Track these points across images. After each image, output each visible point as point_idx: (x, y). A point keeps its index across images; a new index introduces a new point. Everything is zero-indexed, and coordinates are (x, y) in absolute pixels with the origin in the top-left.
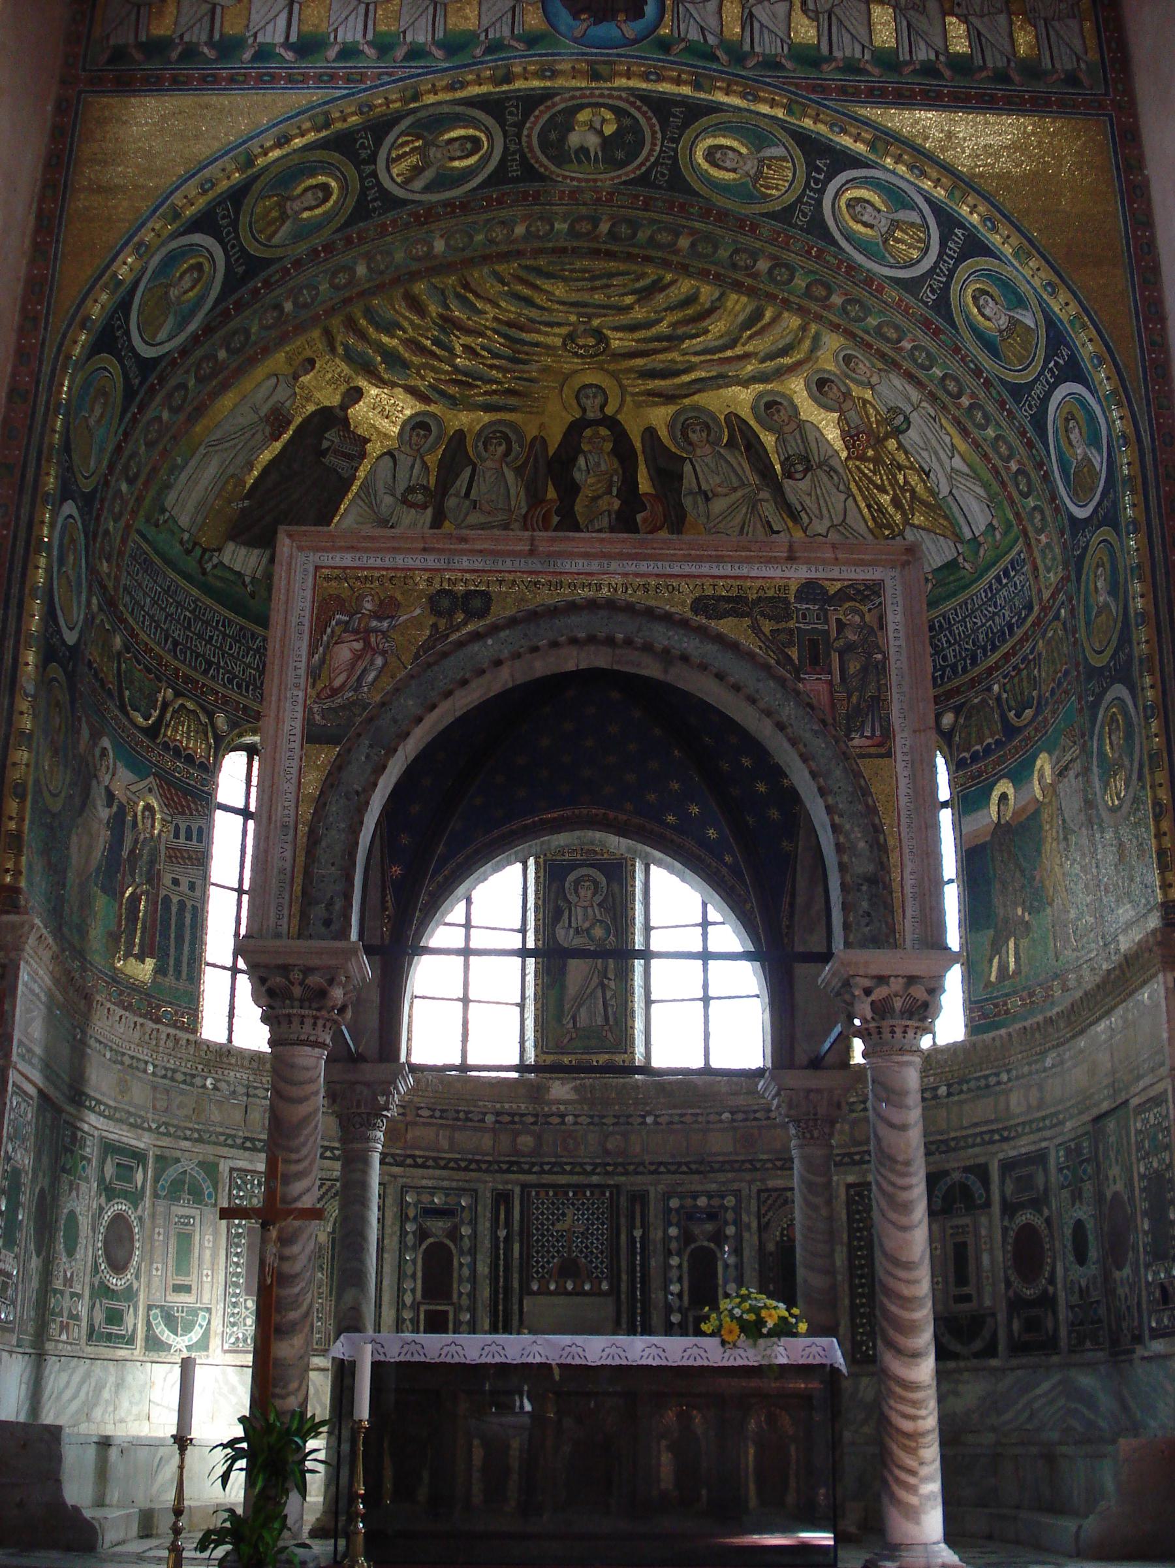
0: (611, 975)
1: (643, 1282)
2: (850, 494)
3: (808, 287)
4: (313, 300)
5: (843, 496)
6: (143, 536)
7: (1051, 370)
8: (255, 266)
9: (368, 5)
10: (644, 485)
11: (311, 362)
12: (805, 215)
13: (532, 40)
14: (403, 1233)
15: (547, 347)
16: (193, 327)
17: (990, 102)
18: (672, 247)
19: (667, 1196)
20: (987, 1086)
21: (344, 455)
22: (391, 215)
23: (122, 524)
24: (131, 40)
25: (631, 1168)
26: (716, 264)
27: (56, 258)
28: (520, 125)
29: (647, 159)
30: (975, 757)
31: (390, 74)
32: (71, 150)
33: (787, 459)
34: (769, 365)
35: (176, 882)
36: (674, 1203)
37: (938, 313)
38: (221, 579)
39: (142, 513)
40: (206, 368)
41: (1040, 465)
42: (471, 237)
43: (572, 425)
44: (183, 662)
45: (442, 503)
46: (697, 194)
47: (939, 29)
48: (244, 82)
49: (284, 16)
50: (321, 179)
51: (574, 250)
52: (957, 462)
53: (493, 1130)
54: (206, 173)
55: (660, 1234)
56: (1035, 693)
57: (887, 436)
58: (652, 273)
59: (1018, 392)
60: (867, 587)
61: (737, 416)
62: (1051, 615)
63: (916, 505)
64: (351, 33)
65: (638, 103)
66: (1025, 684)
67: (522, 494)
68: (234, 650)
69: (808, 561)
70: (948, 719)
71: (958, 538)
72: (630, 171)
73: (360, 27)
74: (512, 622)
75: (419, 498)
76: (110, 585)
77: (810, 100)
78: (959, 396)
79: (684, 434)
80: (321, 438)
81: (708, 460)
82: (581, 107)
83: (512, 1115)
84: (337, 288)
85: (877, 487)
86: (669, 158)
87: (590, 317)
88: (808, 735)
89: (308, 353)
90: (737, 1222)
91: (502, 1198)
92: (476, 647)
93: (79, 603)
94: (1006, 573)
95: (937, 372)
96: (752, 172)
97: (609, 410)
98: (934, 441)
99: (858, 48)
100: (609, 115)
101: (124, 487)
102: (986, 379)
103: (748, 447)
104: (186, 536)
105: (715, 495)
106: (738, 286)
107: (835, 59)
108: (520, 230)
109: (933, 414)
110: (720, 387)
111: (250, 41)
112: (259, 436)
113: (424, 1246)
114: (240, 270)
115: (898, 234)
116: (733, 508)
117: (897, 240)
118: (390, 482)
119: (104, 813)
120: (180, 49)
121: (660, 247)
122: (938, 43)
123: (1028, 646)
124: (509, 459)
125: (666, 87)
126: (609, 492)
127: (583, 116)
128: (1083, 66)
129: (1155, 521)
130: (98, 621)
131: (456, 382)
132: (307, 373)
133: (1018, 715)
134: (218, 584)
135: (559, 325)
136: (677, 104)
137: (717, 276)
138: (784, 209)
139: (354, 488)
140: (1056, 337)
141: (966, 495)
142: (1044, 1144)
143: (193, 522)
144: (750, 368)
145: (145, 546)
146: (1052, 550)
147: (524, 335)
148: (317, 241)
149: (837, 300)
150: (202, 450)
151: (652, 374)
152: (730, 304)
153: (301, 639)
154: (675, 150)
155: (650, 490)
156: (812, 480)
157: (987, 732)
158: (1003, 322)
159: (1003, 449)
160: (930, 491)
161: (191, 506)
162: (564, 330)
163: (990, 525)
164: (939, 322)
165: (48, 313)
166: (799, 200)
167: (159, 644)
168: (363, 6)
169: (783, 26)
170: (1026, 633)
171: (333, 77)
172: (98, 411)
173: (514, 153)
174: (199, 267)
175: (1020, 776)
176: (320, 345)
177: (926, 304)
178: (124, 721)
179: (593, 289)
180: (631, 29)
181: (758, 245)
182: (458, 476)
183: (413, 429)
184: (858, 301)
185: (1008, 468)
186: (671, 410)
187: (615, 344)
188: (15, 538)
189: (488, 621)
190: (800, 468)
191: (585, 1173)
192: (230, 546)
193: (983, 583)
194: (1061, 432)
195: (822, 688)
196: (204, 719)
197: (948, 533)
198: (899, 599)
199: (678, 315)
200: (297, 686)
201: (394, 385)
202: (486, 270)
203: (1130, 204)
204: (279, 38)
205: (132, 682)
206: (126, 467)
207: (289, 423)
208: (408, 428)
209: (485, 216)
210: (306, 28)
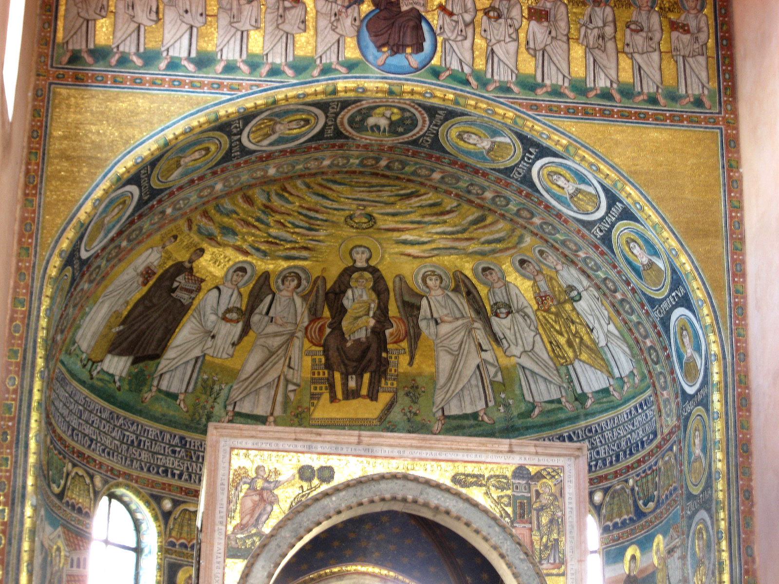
2: (538, 333)
3: (518, 210)
5: (533, 334)
8: (154, 193)
9: (242, 32)
10: (393, 310)
11: (175, 237)
12: (519, 174)
13: (351, 66)
15: (333, 222)
17: (644, 118)
18: (428, 177)
21: (186, 290)
22: (244, 158)
24: (84, 47)
26: (456, 188)
27: (39, 206)
28: (337, 114)
29: (418, 133)
31: (258, 86)
32: (46, 127)
33: (496, 304)
34: (487, 248)
37: (604, 243)
38: (101, 380)
39: (64, 348)
41: (665, 349)
42: (294, 167)
43: (346, 270)
44: (77, 442)
46: (449, 153)
47: (614, 65)
48: (160, 85)
49: (186, 37)
51: (361, 173)
52: (612, 328)
54: (138, 151)
56: (656, 493)
57: (565, 302)
59: (653, 302)
60: (554, 471)
61: (462, 273)
63: (583, 349)
64: (231, 53)
65: (416, 106)
66: (650, 485)
67: (306, 314)
68: (107, 428)
69: (520, 453)
70: (598, 497)
71: (611, 374)
72: (407, 137)
74: (347, 486)
75: (234, 316)
77: (529, 115)
78: (615, 291)
81: (440, 298)
82: (379, 106)
87: (365, 207)
88: (517, 562)
89: (175, 233)
92: (326, 501)
94: (641, 405)
95: (601, 275)
96: (487, 147)
97: (373, 263)
98: (597, 313)
99: (561, 77)
100: (395, 110)
103: (469, 293)
105: (443, 322)
106: (470, 202)
107: (545, 86)
108: (326, 163)
109: (597, 295)
110: (452, 254)
111: (165, 54)
112: (135, 285)
114: (146, 198)
116: (455, 331)
117: (579, 199)
118: (215, 305)
120: (117, 57)
121: (419, 176)
122: (613, 73)
123: (653, 460)
125: (436, 102)
127: (378, 111)
128: (706, 92)
129: (731, 411)
131: (267, 242)
132: (171, 242)
134: (100, 384)
135: (343, 210)
137: (457, 195)
138: (506, 169)
139: (190, 312)
140: (677, 282)
141: (617, 349)
143: (89, 346)
144: (473, 247)
147: (317, 215)
148: (195, 176)
149: (537, 221)
150: (100, 300)
152: (463, 211)
153: (223, 494)
155: (398, 315)
156: (512, 321)
157: (624, 510)
158: (645, 260)
160: (593, 341)
161: (89, 336)
162: (347, 213)
165: (36, 245)
166: (517, 165)
168: (239, 33)
169: (513, 60)
170: (652, 451)
171: (220, 86)
174: (124, 202)
175: (645, 544)
176: (185, 228)
177: (596, 236)
179: (369, 192)
180: (415, 60)
181: (486, 184)
182: (262, 301)
183: (235, 271)
184: (551, 225)
185: (645, 343)
186: (416, 264)
187: (381, 224)
188: (21, 400)
189: (333, 484)
190: (504, 310)
192: (109, 357)
193: (625, 408)
194: (678, 336)
195: (526, 532)
196: (88, 480)
197: (604, 370)
198: (573, 479)
199: (428, 211)
200: (221, 523)
201: (225, 245)
202: (299, 183)
203: (730, 192)
204: (184, 54)
207: (154, 273)
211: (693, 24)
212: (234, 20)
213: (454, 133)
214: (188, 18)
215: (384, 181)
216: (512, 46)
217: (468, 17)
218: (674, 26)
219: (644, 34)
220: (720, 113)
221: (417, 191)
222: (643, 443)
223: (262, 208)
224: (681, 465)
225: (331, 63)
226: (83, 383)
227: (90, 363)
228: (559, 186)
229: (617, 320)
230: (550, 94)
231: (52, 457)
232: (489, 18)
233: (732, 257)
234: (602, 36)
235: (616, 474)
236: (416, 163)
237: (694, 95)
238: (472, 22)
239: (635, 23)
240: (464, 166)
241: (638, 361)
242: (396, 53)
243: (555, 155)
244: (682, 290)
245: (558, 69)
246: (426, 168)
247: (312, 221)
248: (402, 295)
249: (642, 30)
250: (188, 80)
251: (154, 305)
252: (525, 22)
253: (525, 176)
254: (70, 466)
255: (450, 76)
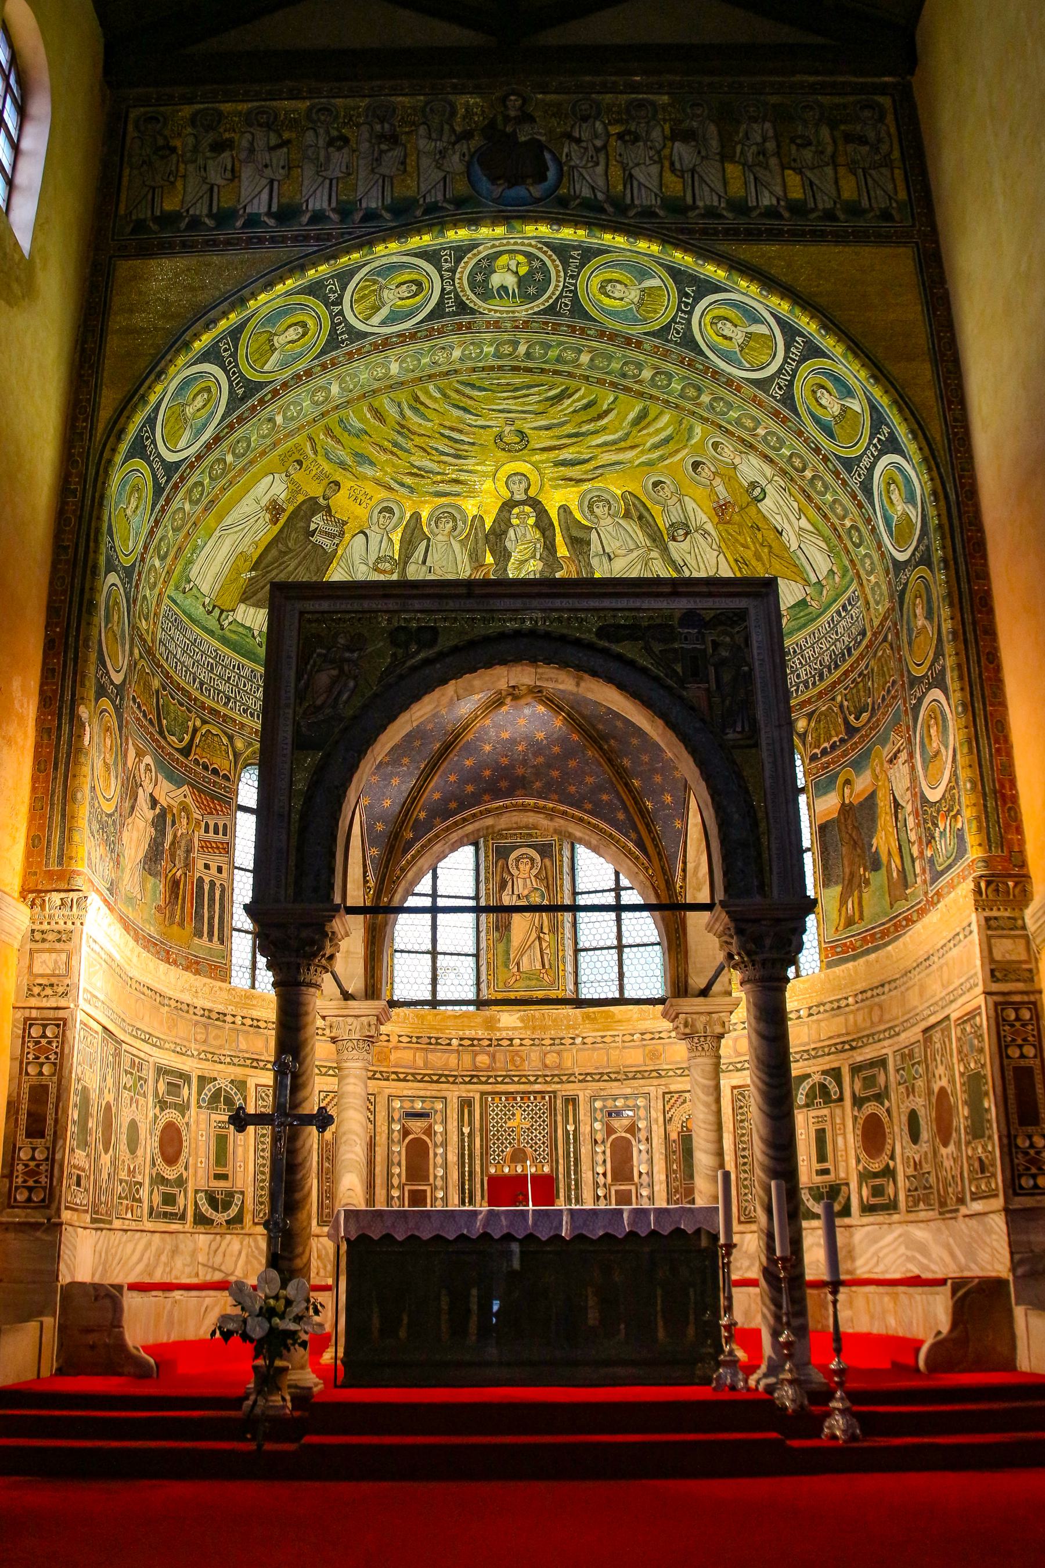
0: (546, 930)
1: (576, 1165)
4: (299, 414)
5: (716, 553)
6: (174, 601)
7: (875, 446)
9: (331, 180)
11: (300, 463)
12: (678, 333)
13: (459, 202)
14: (390, 1131)
16: (207, 435)
19: (593, 1099)
20: (839, 1007)
23: (157, 591)
25: (564, 1078)
28: (453, 271)
29: (553, 293)
30: (824, 752)
31: (350, 233)
35: (207, 867)
36: (598, 1104)
40: (218, 469)
43: (504, 504)
45: (404, 569)
46: (595, 320)
49: (266, 191)
50: (301, 318)
52: (804, 523)
53: (458, 1051)
55: (588, 1129)
56: (869, 700)
58: (561, 384)
59: (849, 464)
62: (881, 638)
64: (319, 202)
68: (248, 687)
71: (807, 582)
72: (539, 304)
73: (326, 198)
76: (149, 639)
78: (804, 470)
79: (590, 507)
80: (309, 521)
81: (610, 528)
82: (500, 254)
83: (472, 1039)
84: (316, 404)
85: (743, 546)
86: (571, 291)
87: (513, 421)
89: (297, 457)
90: (649, 1119)
91: (466, 1103)
93: (124, 652)
94: (844, 607)
96: (636, 300)
97: (532, 493)
98: (786, 508)
99: (715, 198)
100: (521, 258)
101: (157, 563)
102: (824, 456)
103: (641, 517)
104: (207, 600)
106: (627, 389)
107: (698, 208)
108: (457, 353)
113: (407, 1141)
114: (241, 391)
115: (752, 343)
119: (150, 815)
123: (862, 664)
124: (455, 533)
126: (534, 557)
128: (894, 205)
130: (139, 667)
133: (857, 719)
134: (234, 637)
136: (575, 248)
137: (613, 384)
141: (812, 548)
142: (884, 1051)
145: (175, 608)
146: (879, 587)
147: (463, 437)
148: (300, 367)
149: (705, 398)
150: (217, 534)
151: (564, 463)
154: (575, 285)
157: (833, 733)
158: (836, 410)
159: (839, 511)
163: (831, 571)
164: (786, 412)
166: (673, 320)
167: (188, 683)
168: (327, 182)
169: (656, 183)
171: (306, 238)
172: (133, 503)
173: (449, 293)
177: (774, 398)
178: (163, 742)
179: (515, 398)
180: (537, 191)
181: (642, 357)
190: (681, 532)
191: (530, 1083)
192: (242, 607)
193: (827, 616)
196: (225, 740)
201: (365, 478)
204: (264, 209)
205: (168, 714)
206: (158, 547)
207: (284, 510)
208: (376, 512)
209: (428, 344)
210: (284, 200)
211: (871, 135)
212: (321, 168)
213: (595, 283)
214: (268, 172)
215: (527, 379)
216: (654, 169)
217: (599, 143)
218: (848, 138)
219: (813, 148)
220: (913, 226)
221: (567, 389)
222: (849, 650)
223: (397, 427)
224: (899, 650)
225: (436, 202)
226: (211, 633)
227: (217, 612)
228: (725, 337)
229: (812, 512)
230: (703, 216)
231: (166, 705)
232: (625, 142)
233: (945, 383)
234: (762, 152)
235: (820, 695)
236: (560, 344)
237: (880, 209)
238: (605, 147)
239: (801, 137)
240: (613, 337)
241: (838, 555)
242: (514, 185)
243: (717, 289)
244: (886, 430)
245: (712, 190)
246: (570, 348)
247: (457, 446)
248: (568, 529)
249: (810, 144)
250: (268, 236)
251: (291, 551)
252: (669, 144)
253: (684, 333)
254: (198, 723)
255: (580, 204)
